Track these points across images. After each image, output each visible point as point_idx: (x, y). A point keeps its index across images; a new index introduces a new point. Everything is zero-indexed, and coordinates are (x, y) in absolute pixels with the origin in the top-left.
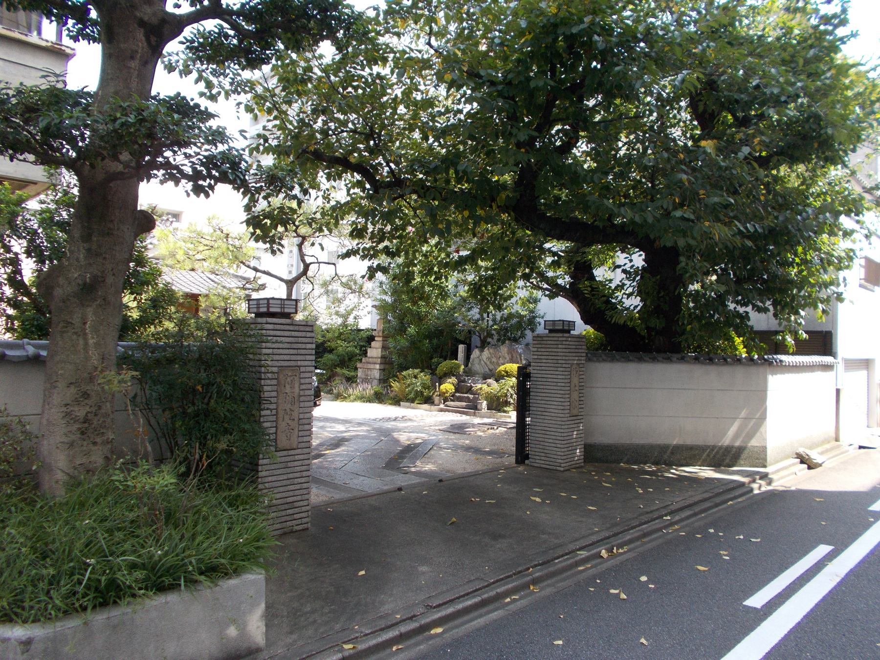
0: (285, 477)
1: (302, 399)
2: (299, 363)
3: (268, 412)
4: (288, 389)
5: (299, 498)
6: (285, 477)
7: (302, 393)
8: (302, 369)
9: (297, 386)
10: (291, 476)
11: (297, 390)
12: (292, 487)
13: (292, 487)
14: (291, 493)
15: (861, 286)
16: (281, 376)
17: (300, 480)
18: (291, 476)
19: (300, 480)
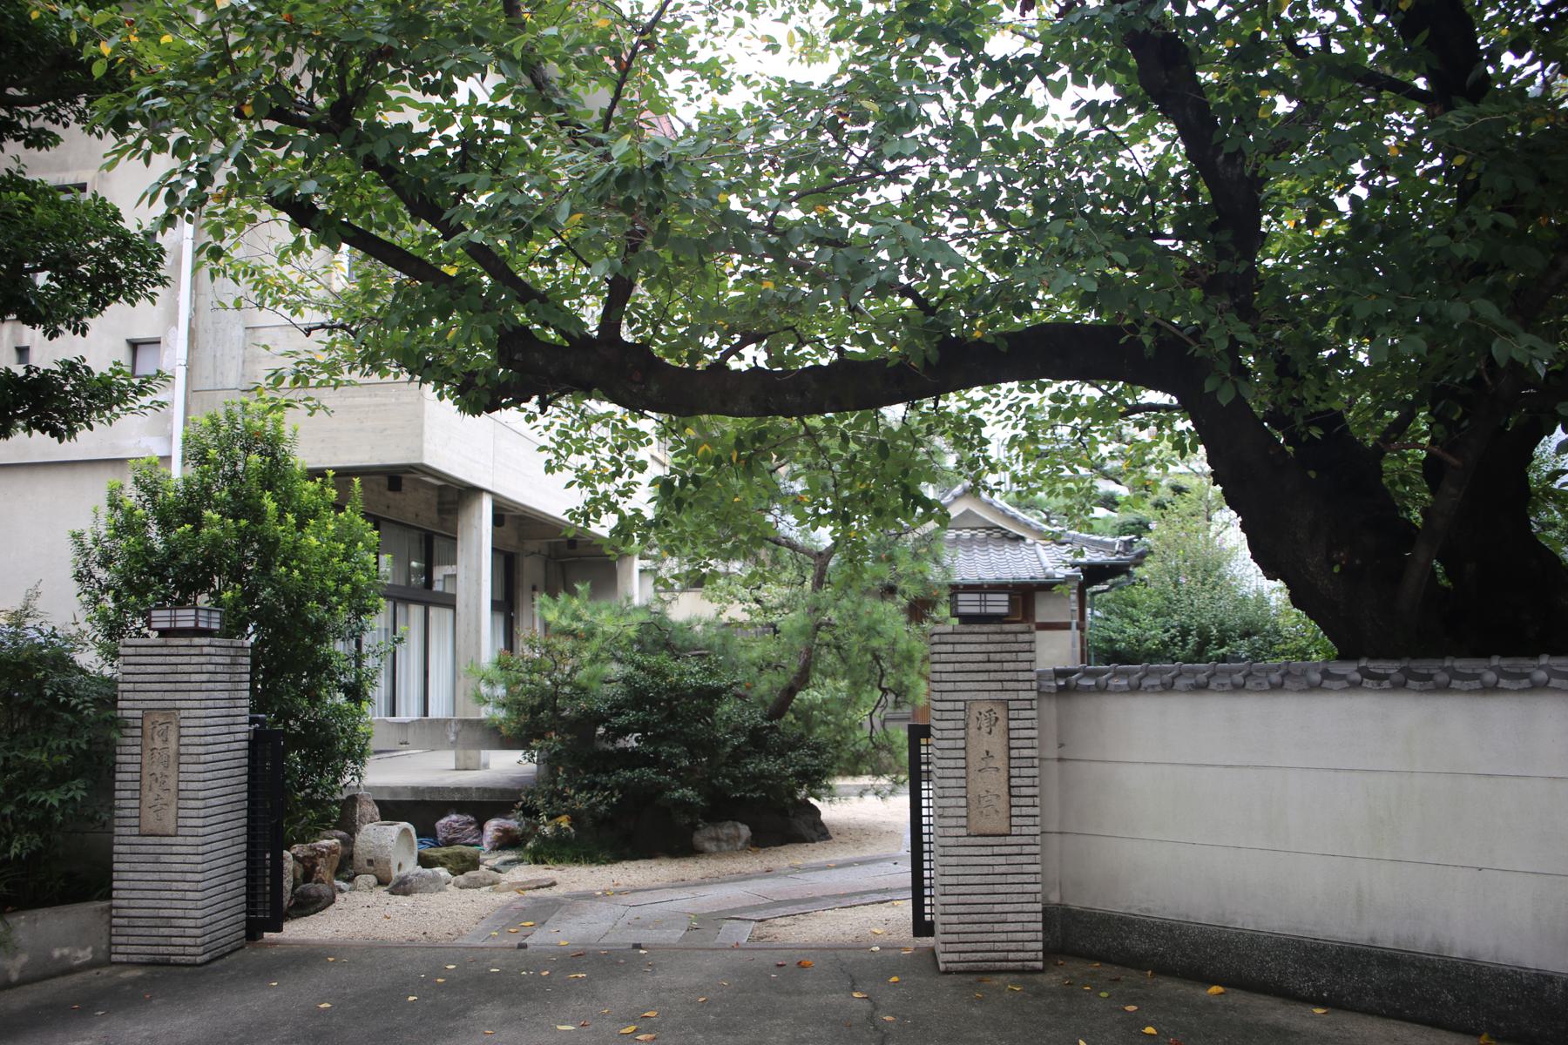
0: (156, 876)
1: (183, 759)
2: (178, 704)
3: (128, 794)
4: (158, 743)
5: (180, 913)
6: (156, 876)
7: (183, 750)
8: (184, 713)
9: (173, 738)
10: (165, 876)
11: (173, 745)
12: (167, 894)
13: (167, 894)
14: (167, 904)
15: (84, 335)
16: (148, 724)
17: (180, 885)
18: (165, 876)
19: (180, 885)
